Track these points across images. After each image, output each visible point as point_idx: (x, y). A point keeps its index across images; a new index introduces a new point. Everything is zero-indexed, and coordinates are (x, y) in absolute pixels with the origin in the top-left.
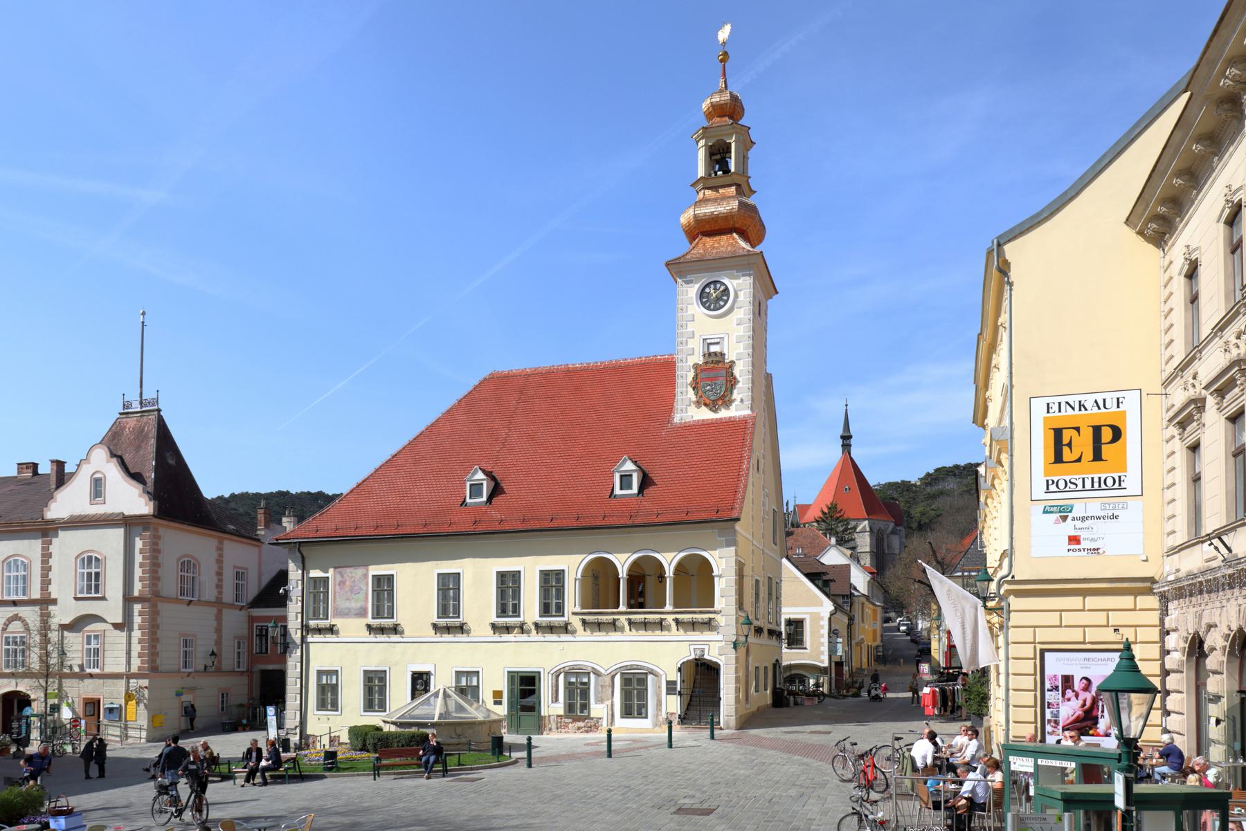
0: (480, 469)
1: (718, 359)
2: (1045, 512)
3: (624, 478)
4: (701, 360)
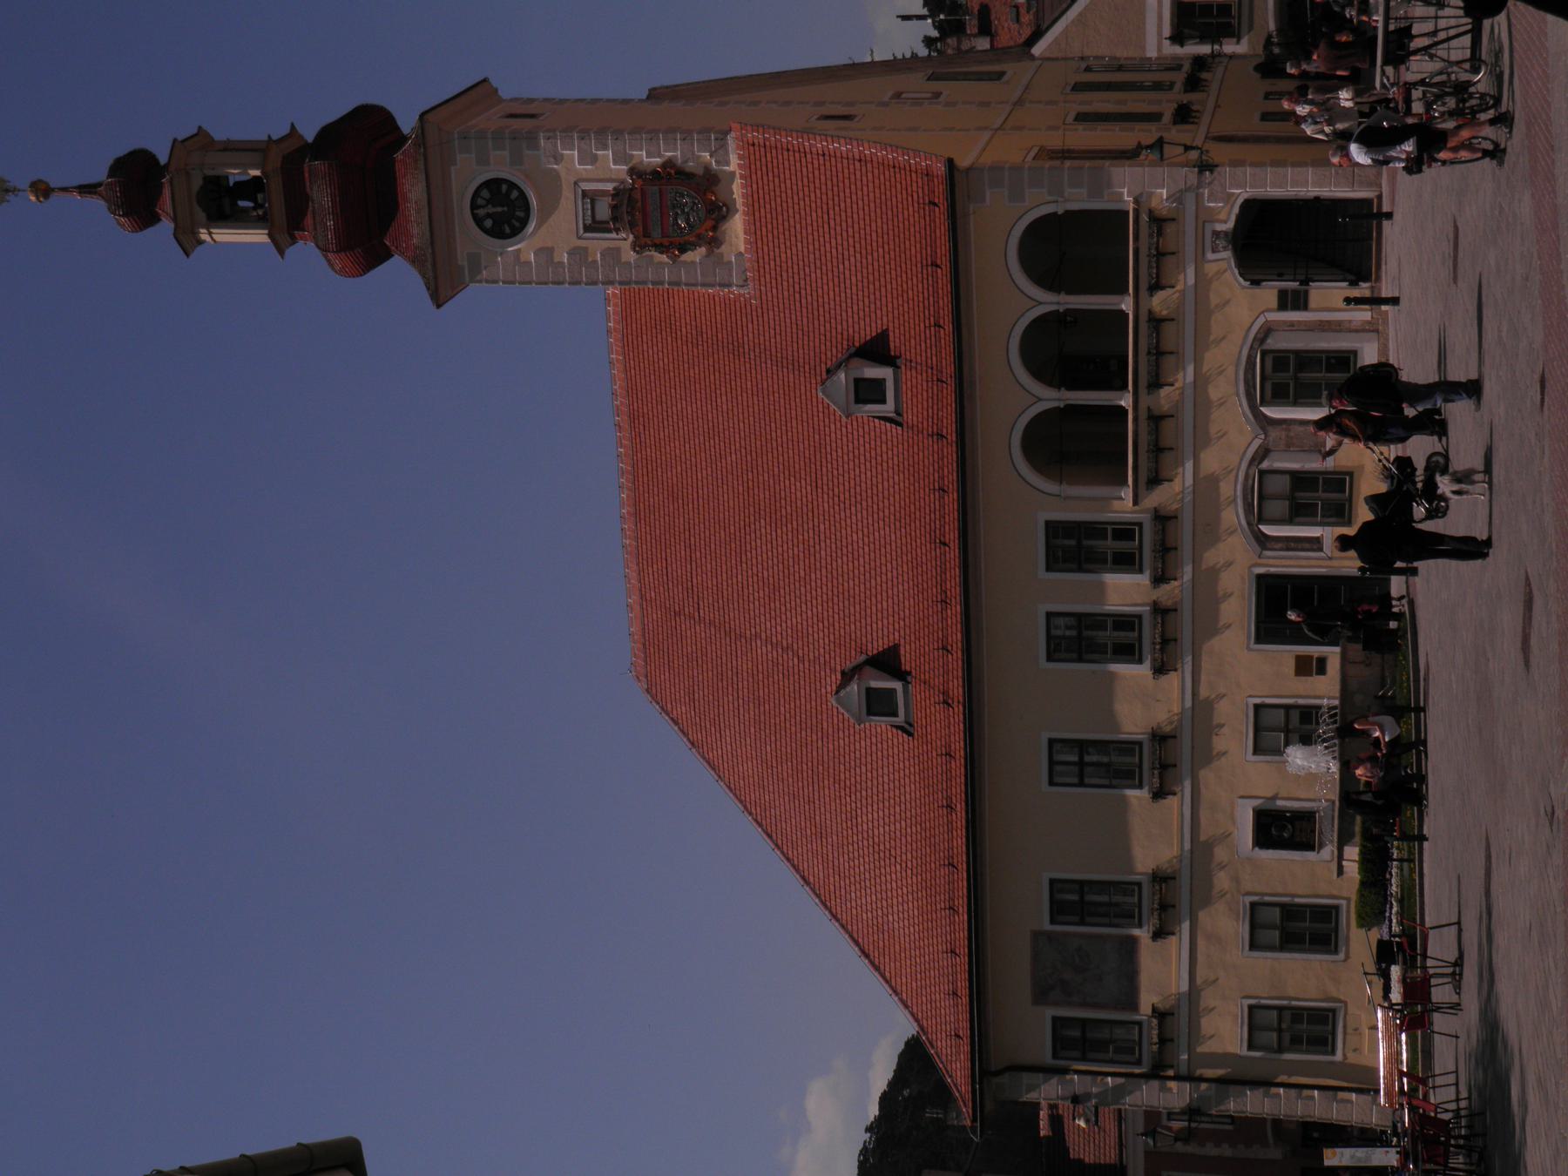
0: (837, 692)
1: (625, 202)
4: (623, 242)
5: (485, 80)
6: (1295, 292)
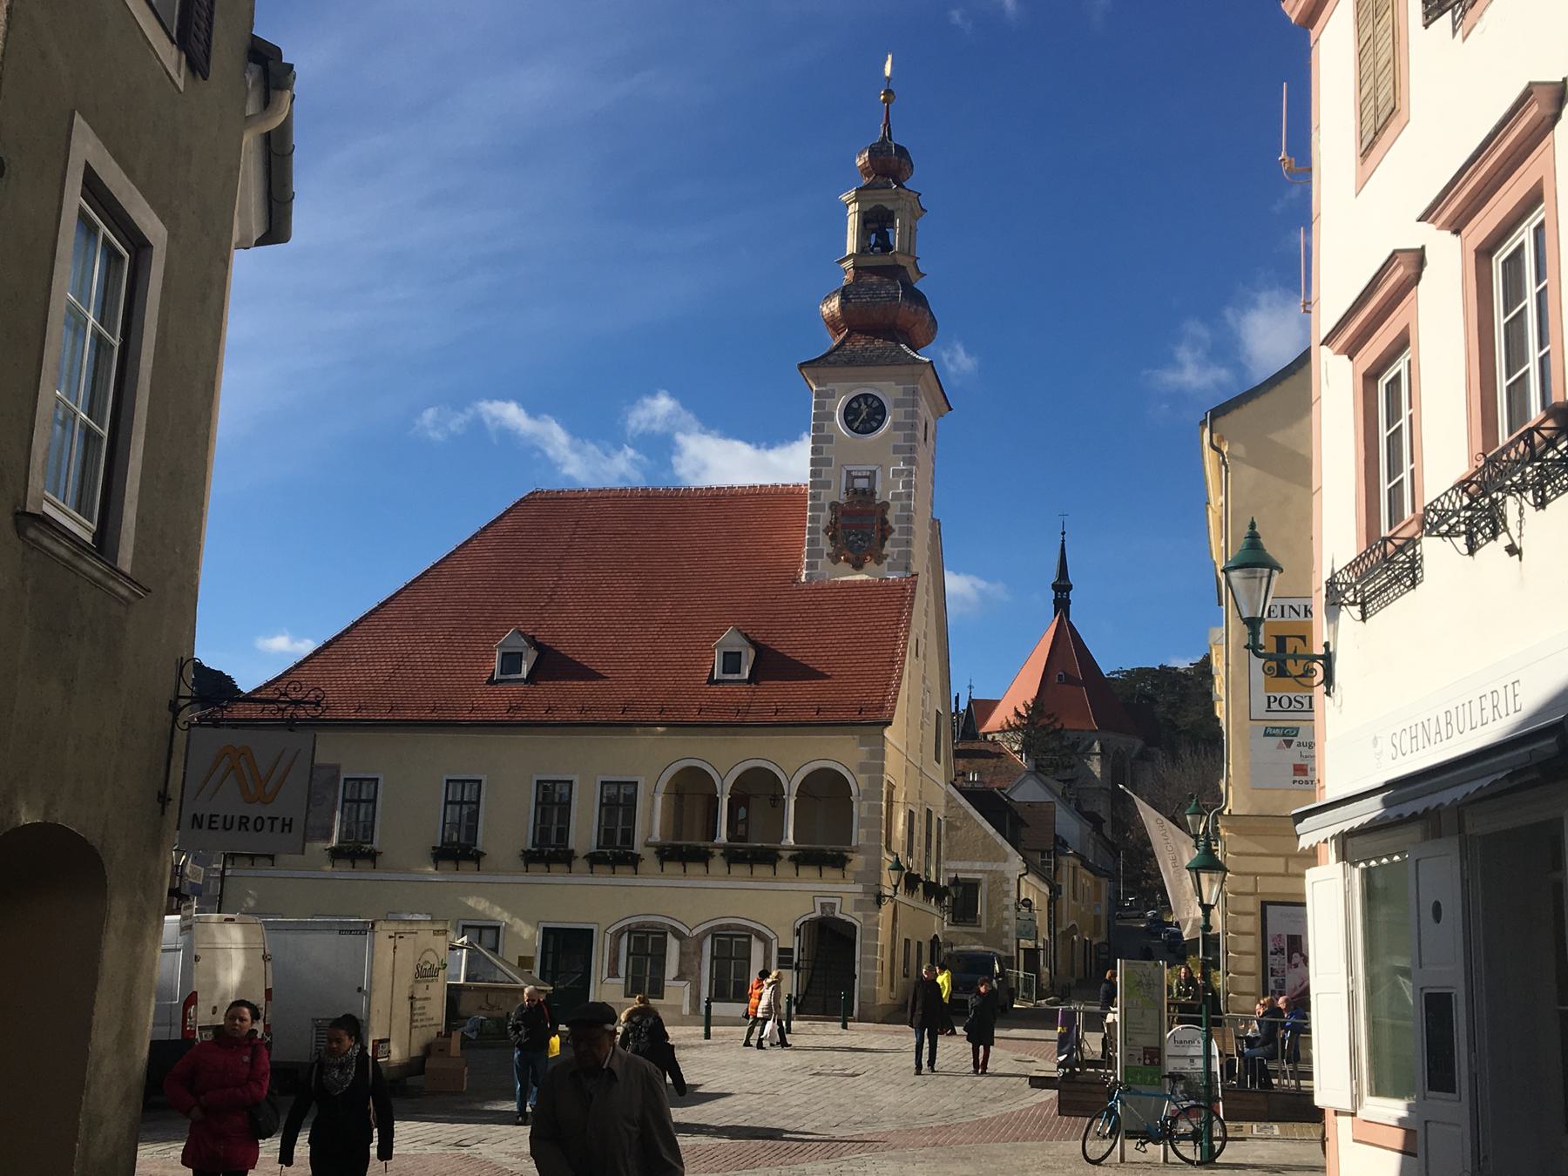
2: (1266, 735)
3: (727, 656)
5: (950, 409)
6: (792, 959)
